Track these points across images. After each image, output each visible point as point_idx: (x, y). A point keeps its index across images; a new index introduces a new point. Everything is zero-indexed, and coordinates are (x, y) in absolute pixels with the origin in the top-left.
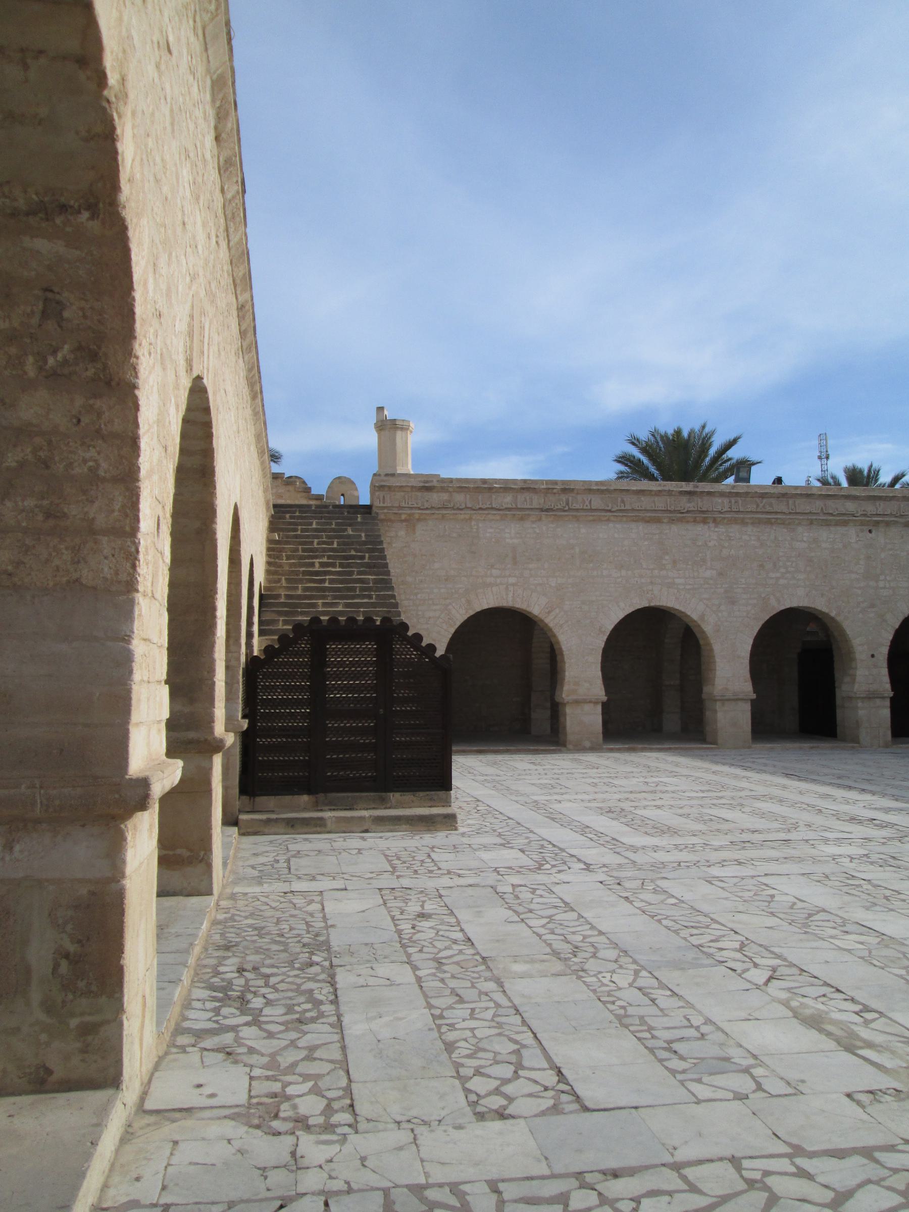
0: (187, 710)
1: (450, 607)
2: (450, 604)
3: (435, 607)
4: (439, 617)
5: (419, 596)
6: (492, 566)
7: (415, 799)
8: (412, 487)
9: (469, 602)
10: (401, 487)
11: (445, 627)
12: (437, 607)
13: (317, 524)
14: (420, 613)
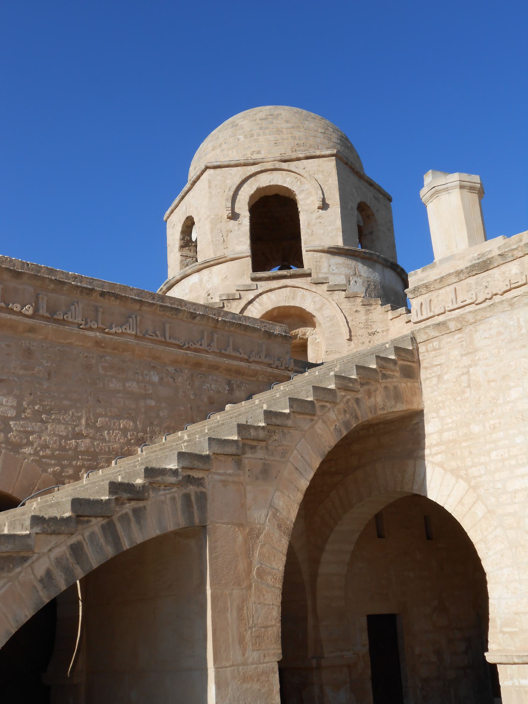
5: (493, 455)
14: (499, 485)
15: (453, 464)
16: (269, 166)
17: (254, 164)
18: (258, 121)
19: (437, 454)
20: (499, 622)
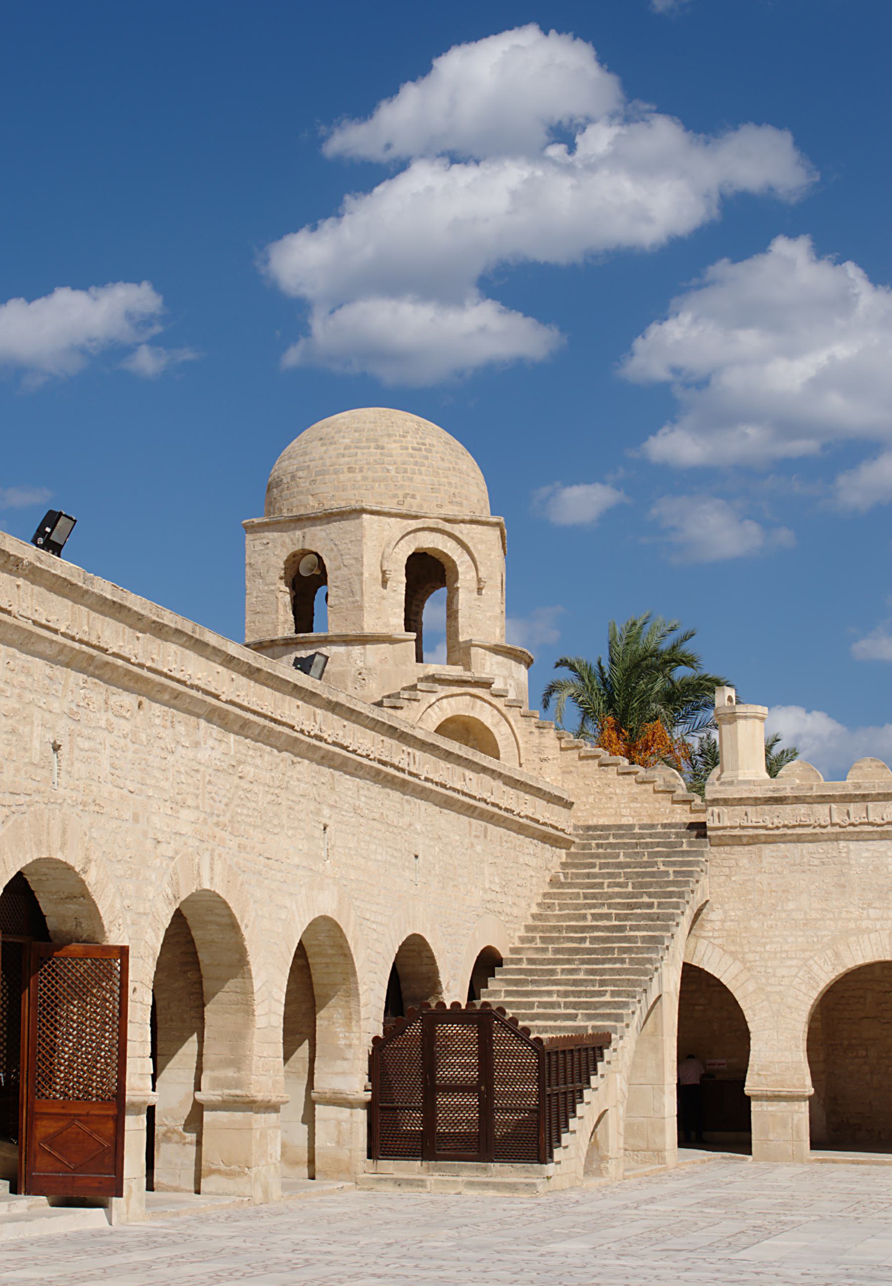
0: (236, 1075)
1: (811, 962)
2: (811, 957)
3: (789, 963)
4: (796, 976)
5: (768, 947)
6: (870, 905)
7: (512, 1169)
8: (756, 799)
9: (837, 955)
10: (741, 799)
11: (803, 988)
12: (795, 962)
13: (625, 855)
14: (770, 970)
15: (733, 948)
16: (430, 523)
17: (416, 517)
18: (411, 451)
19: (719, 937)
20: (756, 1068)
